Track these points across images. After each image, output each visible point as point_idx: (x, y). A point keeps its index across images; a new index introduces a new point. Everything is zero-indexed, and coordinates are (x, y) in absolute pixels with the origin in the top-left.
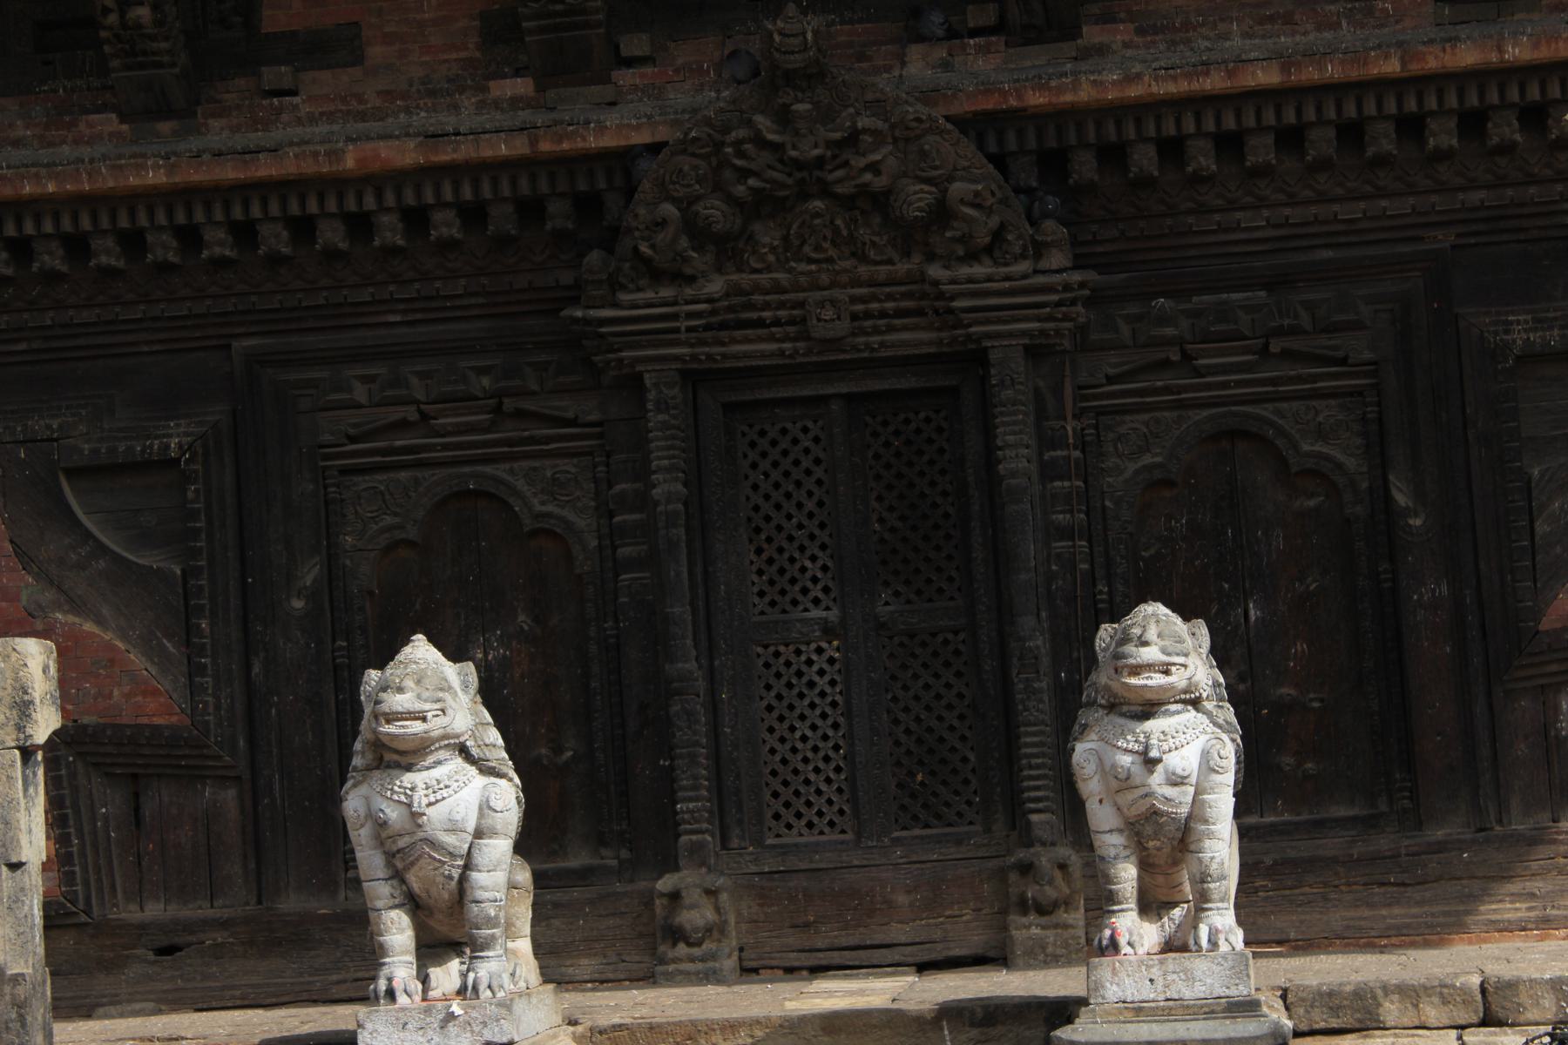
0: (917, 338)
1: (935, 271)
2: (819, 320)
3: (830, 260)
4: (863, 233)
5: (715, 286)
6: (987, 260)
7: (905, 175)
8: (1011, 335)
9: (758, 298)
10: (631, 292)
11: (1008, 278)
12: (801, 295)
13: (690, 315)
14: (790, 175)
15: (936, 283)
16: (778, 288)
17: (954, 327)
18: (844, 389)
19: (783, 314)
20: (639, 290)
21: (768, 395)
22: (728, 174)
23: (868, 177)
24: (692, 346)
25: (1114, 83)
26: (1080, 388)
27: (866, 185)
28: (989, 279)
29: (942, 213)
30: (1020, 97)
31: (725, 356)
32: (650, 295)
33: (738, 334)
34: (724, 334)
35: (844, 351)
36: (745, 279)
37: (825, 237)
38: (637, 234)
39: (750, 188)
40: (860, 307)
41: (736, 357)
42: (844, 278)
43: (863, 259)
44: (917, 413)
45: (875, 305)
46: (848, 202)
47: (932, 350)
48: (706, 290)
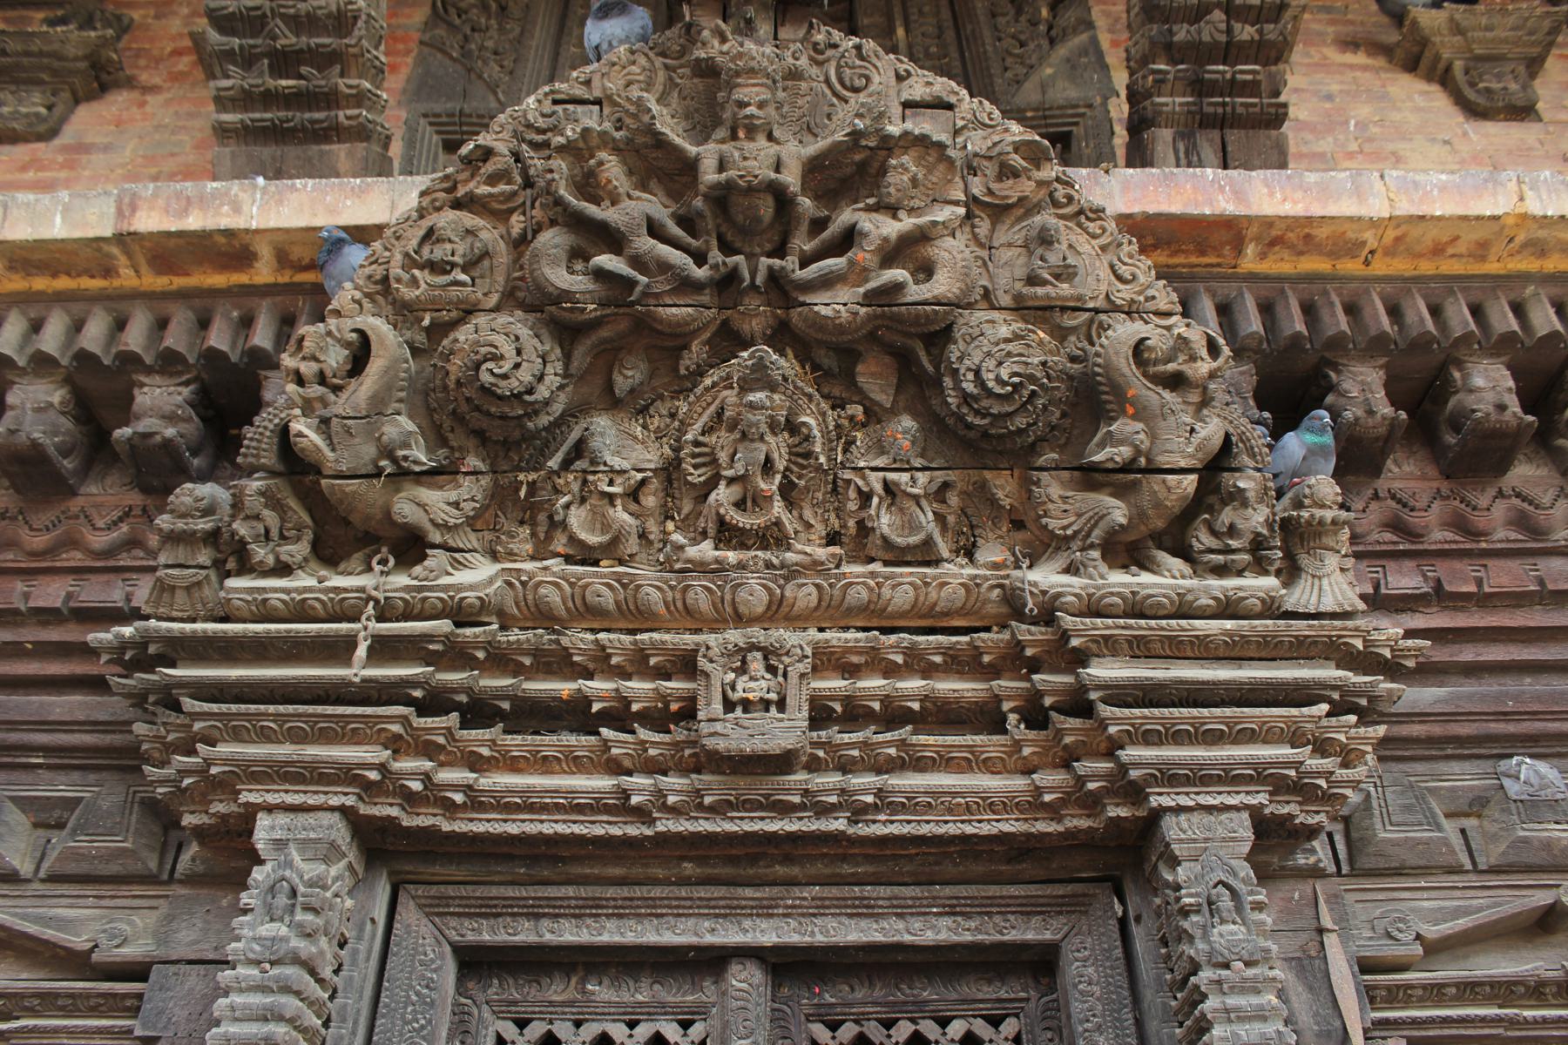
0: (973, 789)
1: (1046, 577)
2: (729, 706)
3: (772, 537)
5: (476, 576)
6: (1176, 563)
8: (1228, 777)
9: (579, 639)
11: (1228, 608)
14: (700, 259)
16: (636, 616)
18: (766, 933)
19: (639, 687)
20: (283, 569)
21: (570, 934)
22: (552, 240)
23: (898, 274)
25: (1443, 188)
26: (1366, 966)
30: (1238, 195)
31: (476, 802)
33: (516, 743)
34: (479, 739)
35: (785, 809)
36: (552, 577)
37: (768, 467)
39: (600, 274)
40: (834, 684)
41: (503, 805)
42: (804, 594)
43: (859, 541)
44: (944, 1023)
45: (873, 683)
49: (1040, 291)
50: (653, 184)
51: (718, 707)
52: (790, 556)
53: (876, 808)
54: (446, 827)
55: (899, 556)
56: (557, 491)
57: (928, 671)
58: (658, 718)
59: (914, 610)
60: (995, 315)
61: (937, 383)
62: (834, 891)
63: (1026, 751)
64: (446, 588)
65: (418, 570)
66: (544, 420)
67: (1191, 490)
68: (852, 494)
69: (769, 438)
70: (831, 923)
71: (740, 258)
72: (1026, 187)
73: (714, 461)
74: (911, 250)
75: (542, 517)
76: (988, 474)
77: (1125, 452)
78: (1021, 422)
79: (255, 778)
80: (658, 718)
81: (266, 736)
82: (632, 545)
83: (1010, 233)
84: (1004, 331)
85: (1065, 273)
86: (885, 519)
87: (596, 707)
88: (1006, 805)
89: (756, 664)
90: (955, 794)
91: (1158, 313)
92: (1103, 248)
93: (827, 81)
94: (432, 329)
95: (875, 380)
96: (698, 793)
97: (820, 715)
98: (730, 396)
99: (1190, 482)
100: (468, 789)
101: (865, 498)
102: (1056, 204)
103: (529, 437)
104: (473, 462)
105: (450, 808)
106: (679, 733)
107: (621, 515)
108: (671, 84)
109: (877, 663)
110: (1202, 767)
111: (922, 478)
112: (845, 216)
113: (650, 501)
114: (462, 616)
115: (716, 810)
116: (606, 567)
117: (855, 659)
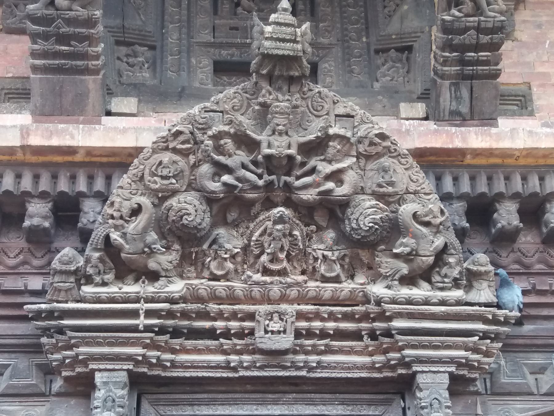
1: (378, 290)
2: (266, 332)
3: (283, 273)
4: (318, 248)
5: (177, 287)
6: (425, 285)
7: (362, 191)
8: (440, 361)
9: (213, 307)
10: (97, 285)
11: (443, 303)
12: (251, 308)
13: (149, 314)
14: (260, 177)
15: (378, 303)
16: (232, 299)
17: (385, 352)
19: (234, 325)
20: (104, 284)
24: (146, 346)
27: (329, 192)
28: (426, 302)
29: (393, 229)
31: (174, 365)
32: (113, 289)
34: (176, 342)
35: (285, 368)
38: (110, 221)
40: (303, 324)
42: (293, 293)
43: (313, 274)
45: (317, 324)
46: (306, 212)
47: (364, 375)
48: (167, 289)
49: (382, 190)
50: (243, 147)
51: (262, 333)
52: (289, 280)
53: (316, 368)
54: (163, 374)
55: (325, 279)
56: (205, 255)
57: (336, 320)
58: (241, 335)
59: (332, 298)
60: (365, 197)
61: (344, 221)
62: (300, 396)
63: (370, 349)
64: (167, 293)
65: (156, 284)
66: (203, 233)
67: (431, 262)
68: (311, 257)
69: (283, 240)
70: (300, 407)
71: (273, 177)
72: (380, 149)
73: (262, 246)
74: (336, 177)
75: (199, 264)
76: (360, 251)
77: (408, 249)
78: (372, 238)
79: (95, 360)
80: (241, 335)
81: (99, 344)
82: (233, 275)
83: (371, 165)
84: (368, 204)
85: (391, 184)
86: (323, 268)
87: (218, 332)
88: (363, 367)
89: (276, 317)
90: (344, 363)
91: (425, 194)
92: (406, 169)
93: (308, 106)
94: (161, 197)
95: (321, 219)
96: (255, 362)
97: (298, 334)
98: (269, 224)
99: (431, 259)
100: (172, 361)
101: (316, 259)
102: (390, 152)
103: (196, 238)
104: (177, 247)
105: (165, 368)
106: (247, 340)
107: (229, 265)
108: (249, 106)
109: (318, 316)
110: (431, 358)
111: (336, 253)
112: (312, 162)
113: (239, 259)
114: (172, 301)
115: (261, 368)
116: (223, 283)
117: (311, 316)
